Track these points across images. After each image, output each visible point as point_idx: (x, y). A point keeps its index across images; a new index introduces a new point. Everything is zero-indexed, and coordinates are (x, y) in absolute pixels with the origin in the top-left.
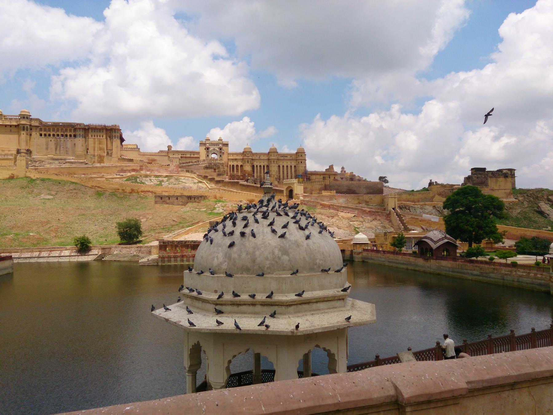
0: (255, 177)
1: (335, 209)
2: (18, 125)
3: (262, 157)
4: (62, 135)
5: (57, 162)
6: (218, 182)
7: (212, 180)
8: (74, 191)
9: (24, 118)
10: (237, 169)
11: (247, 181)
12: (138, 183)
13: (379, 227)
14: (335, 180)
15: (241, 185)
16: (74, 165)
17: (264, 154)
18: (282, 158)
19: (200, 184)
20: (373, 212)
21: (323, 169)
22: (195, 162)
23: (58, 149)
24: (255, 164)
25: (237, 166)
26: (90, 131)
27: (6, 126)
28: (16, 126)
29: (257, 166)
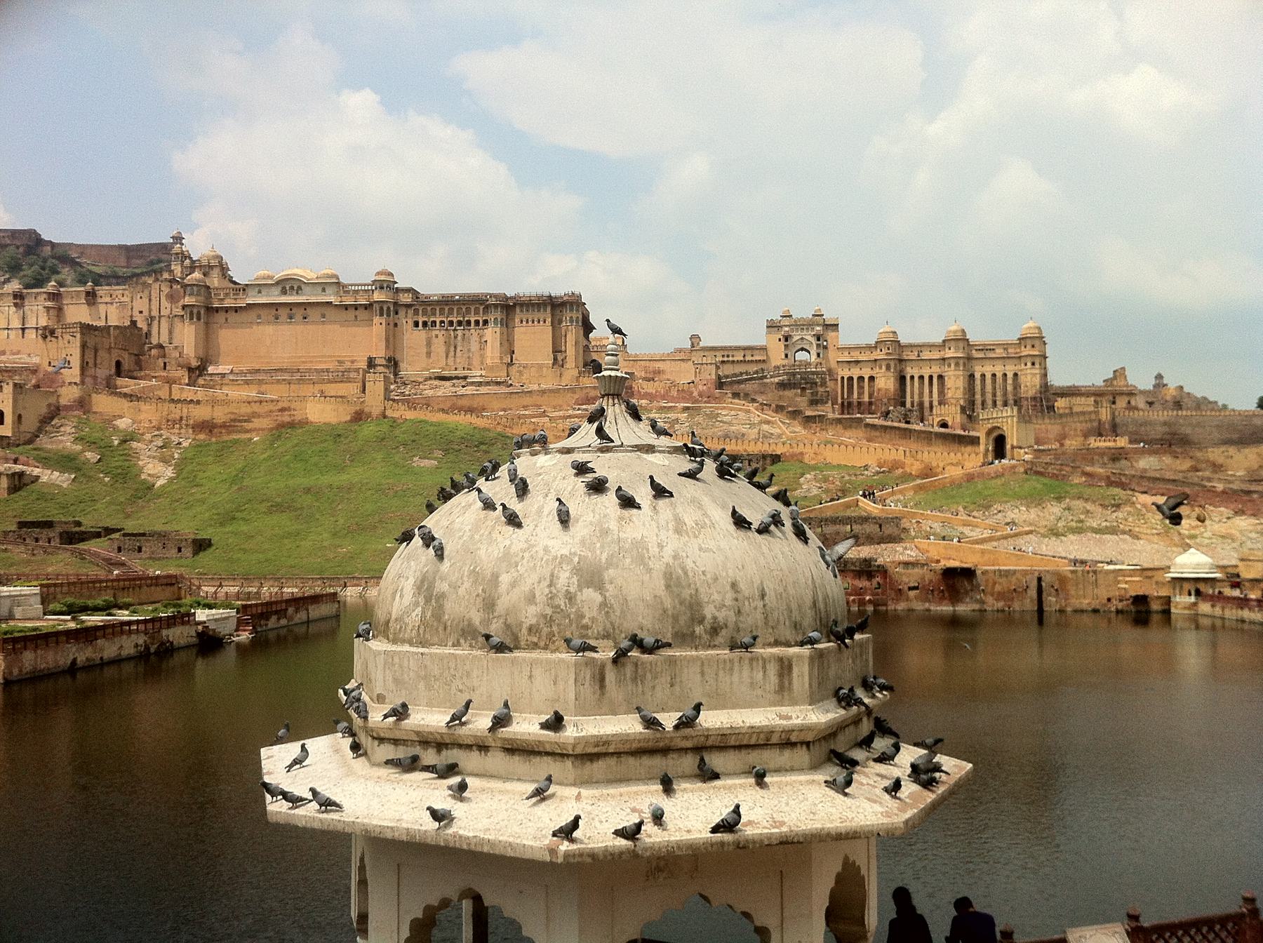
0: (908, 405)
1: (1123, 486)
2: (371, 305)
3: (926, 355)
4: (460, 323)
5: (448, 383)
6: (809, 420)
7: (795, 414)
8: (483, 447)
9: (382, 288)
10: (861, 388)
11: (886, 415)
13: (1253, 535)
14: (1130, 407)
15: (867, 425)
16: (484, 390)
17: (931, 346)
18: (981, 355)
19: (765, 427)
20: (1235, 492)
21: (1094, 377)
22: (756, 372)
24: (910, 371)
25: (861, 379)
26: (518, 310)
27: (346, 307)
28: (366, 307)
29: (912, 377)
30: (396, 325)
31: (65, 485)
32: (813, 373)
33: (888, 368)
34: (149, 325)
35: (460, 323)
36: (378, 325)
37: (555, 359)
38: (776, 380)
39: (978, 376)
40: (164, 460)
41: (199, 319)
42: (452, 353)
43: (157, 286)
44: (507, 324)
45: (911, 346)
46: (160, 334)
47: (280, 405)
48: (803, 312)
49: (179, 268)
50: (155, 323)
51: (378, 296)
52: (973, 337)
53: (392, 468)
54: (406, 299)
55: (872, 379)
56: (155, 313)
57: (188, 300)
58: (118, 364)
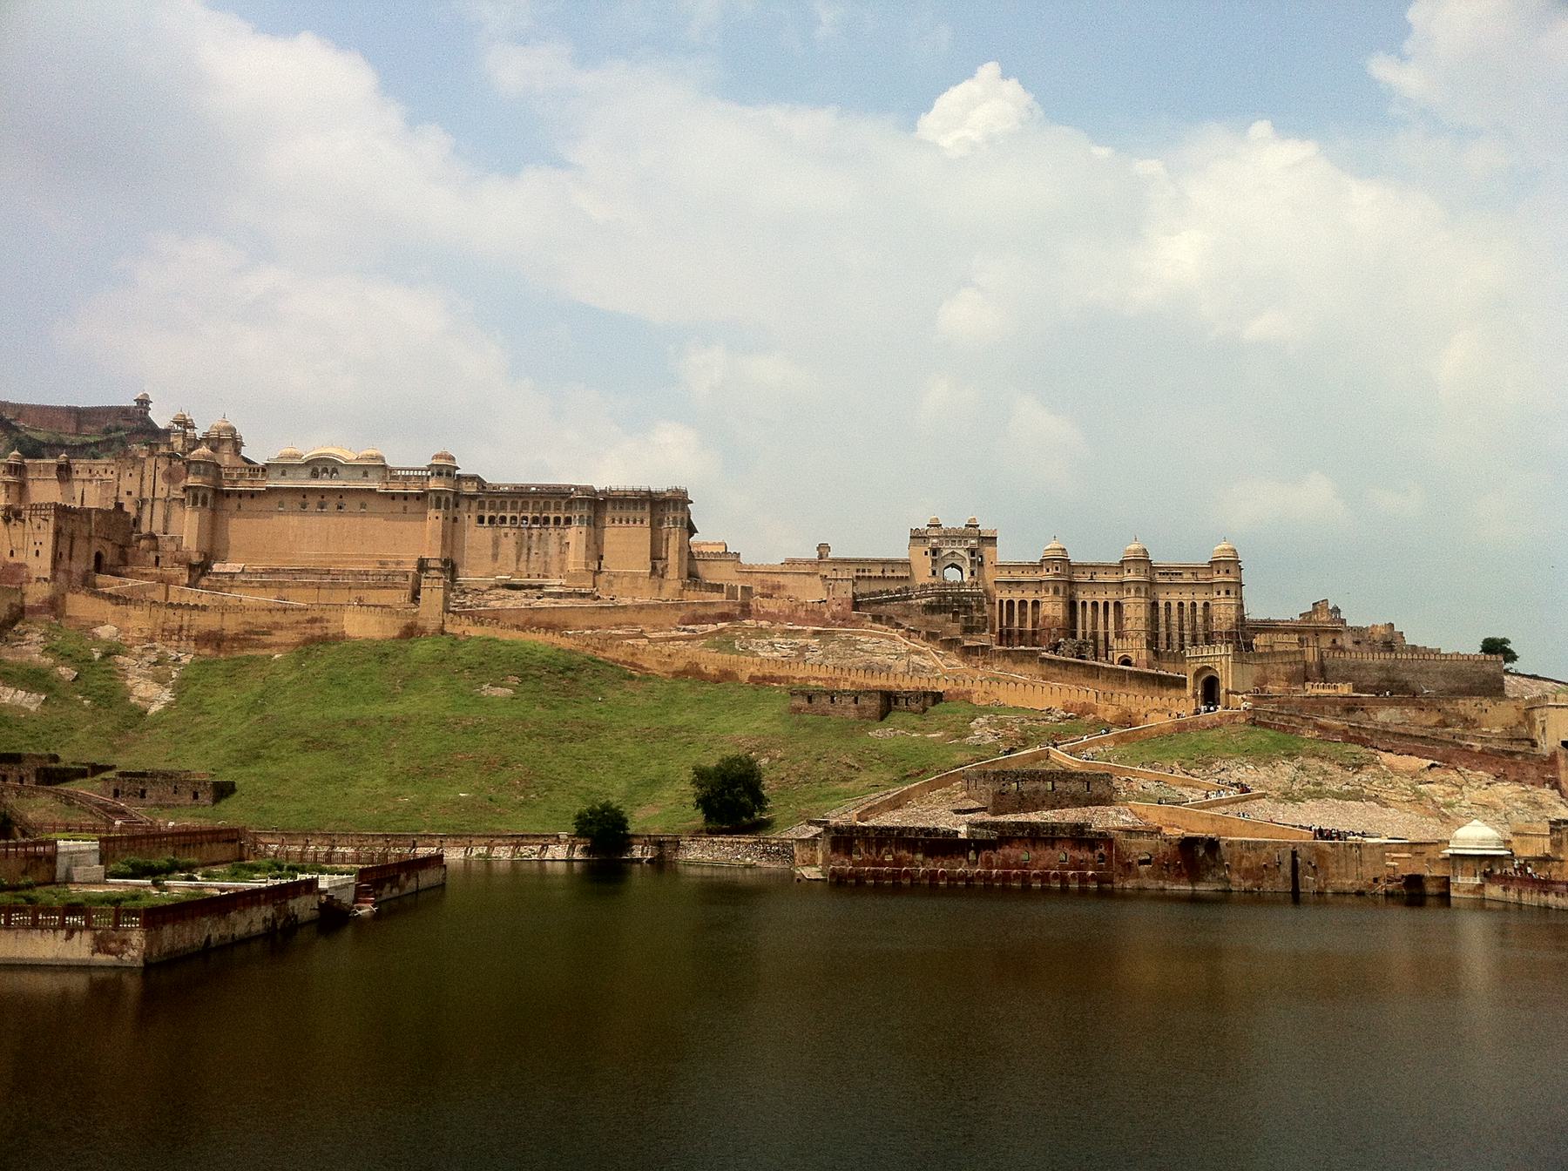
0: (1080, 636)
1: (1364, 743)
2: (425, 495)
3: (1101, 577)
4: (535, 520)
5: (519, 594)
6: (968, 652)
7: (950, 644)
8: (570, 674)
9: (440, 474)
10: (1023, 614)
11: (1055, 648)
12: (735, 652)
13: (1519, 804)
14: (1335, 647)
15: (1043, 660)
16: (565, 603)
17: (1107, 568)
18: (1165, 580)
19: (915, 658)
20: (1495, 753)
21: (1289, 610)
22: (899, 591)
23: (524, 557)
24: (1081, 596)
25: (1023, 603)
26: (609, 507)
27: (393, 496)
28: (418, 497)
29: (1084, 604)
30: (455, 520)
31: (33, 708)
32: (967, 594)
33: (1056, 591)
34: (139, 510)
35: (535, 520)
36: (433, 521)
37: (654, 568)
38: (923, 601)
39: (1162, 604)
40: (161, 681)
41: (204, 503)
42: (524, 557)
43: (151, 461)
44: (595, 526)
45: (1083, 566)
46: (152, 521)
47: (309, 616)
48: (954, 521)
49: (180, 441)
50: (147, 508)
51: (433, 484)
52: (1156, 559)
53: (456, 697)
54: (469, 488)
55: (1036, 604)
56: (147, 495)
57: (191, 481)
58: (99, 557)
